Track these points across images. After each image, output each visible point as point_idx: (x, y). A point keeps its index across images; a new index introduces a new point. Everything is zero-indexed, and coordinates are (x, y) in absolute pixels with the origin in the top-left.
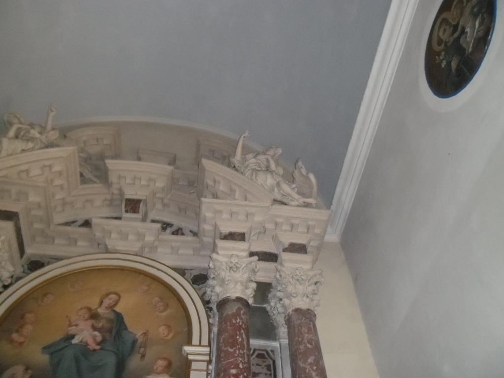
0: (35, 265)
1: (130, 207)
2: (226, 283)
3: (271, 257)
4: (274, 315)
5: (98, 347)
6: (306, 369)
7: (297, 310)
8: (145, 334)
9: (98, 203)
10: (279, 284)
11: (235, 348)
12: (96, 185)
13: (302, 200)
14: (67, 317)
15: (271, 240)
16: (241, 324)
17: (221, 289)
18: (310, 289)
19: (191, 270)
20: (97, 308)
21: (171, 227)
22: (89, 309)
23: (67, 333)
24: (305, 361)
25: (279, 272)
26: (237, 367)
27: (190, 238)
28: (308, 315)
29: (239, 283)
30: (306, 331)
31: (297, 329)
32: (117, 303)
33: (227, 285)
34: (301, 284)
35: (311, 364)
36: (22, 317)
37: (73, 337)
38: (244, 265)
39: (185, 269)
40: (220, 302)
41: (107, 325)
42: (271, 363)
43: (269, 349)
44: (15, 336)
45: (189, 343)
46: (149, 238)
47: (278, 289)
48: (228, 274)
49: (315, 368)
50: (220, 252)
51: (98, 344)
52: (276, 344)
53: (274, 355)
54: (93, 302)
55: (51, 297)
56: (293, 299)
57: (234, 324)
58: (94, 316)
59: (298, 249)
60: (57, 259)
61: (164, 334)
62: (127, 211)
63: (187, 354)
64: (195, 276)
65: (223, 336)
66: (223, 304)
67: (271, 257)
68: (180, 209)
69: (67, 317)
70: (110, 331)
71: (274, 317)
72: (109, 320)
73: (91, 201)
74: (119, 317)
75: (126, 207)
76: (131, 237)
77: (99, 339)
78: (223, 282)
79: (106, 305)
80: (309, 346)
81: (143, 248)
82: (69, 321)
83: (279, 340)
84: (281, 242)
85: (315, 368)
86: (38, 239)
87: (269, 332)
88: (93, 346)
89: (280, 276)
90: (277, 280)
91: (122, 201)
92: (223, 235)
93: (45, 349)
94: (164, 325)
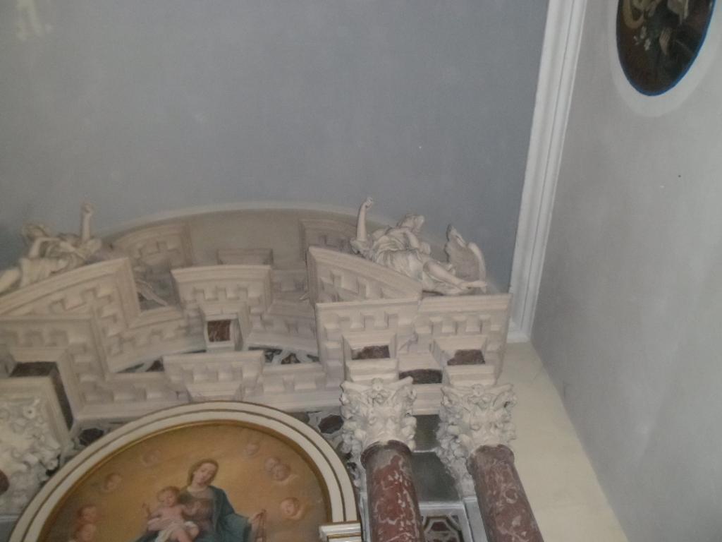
0: (90, 435)
1: (216, 333)
2: (371, 422)
3: (433, 377)
4: (450, 462)
6: (511, 536)
7: (484, 450)
8: (262, 515)
9: (169, 334)
10: (450, 413)
11: (398, 518)
12: (163, 309)
13: (465, 285)
14: (144, 505)
15: (428, 351)
16: (401, 480)
17: (364, 433)
18: (498, 415)
19: (316, 412)
20: (186, 487)
21: (279, 354)
22: (175, 490)
23: (147, 530)
24: (508, 526)
25: (447, 396)
27: (307, 366)
28: (501, 455)
29: (390, 421)
30: (502, 479)
31: (487, 477)
32: (213, 475)
33: (371, 425)
34: (482, 409)
35: (517, 528)
36: (80, 514)
37: (155, 534)
38: (393, 393)
39: (308, 412)
40: (365, 452)
41: (205, 510)
42: (456, 536)
43: (450, 515)
45: (328, 520)
46: (249, 374)
47: (450, 421)
48: (371, 409)
49: (524, 533)
50: (356, 378)
52: (459, 506)
53: (457, 521)
54: (180, 479)
55: (117, 479)
56: (475, 434)
57: (392, 483)
58: (183, 499)
60: (120, 423)
61: (289, 512)
62: (212, 340)
63: (328, 538)
64: (323, 420)
65: (378, 503)
66: (370, 454)
67: (433, 377)
68: (288, 326)
69: (144, 505)
70: (210, 518)
71: (450, 465)
72: (206, 502)
73: (159, 333)
74: (220, 496)
75: (209, 333)
76: (222, 376)
78: (365, 423)
79: (199, 481)
80: (510, 501)
81: (241, 389)
82: (148, 510)
83: (462, 498)
84: (443, 352)
85: (524, 533)
86: (90, 398)
87: (445, 488)
89: (450, 401)
90: (446, 408)
91: (203, 325)
92: (356, 353)
94: (287, 499)
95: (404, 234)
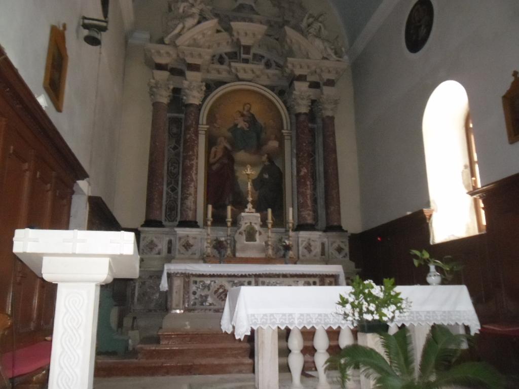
5: (248, 130)
7: (328, 117)
8: (265, 124)
22: (240, 112)
26: (305, 143)
28: (332, 119)
32: (250, 109)
44: (215, 125)
46: (258, 73)
51: (248, 128)
52: (315, 126)
54: (240, 108)
58: (243, 115)
59: (330, 83)
62: (244, 54)
66: (298, 115)
74: (253, 116)
77: (247, 125)
88: (246, 129)
91: (240, 48)
93: (229, 130)
95: (320, 27)
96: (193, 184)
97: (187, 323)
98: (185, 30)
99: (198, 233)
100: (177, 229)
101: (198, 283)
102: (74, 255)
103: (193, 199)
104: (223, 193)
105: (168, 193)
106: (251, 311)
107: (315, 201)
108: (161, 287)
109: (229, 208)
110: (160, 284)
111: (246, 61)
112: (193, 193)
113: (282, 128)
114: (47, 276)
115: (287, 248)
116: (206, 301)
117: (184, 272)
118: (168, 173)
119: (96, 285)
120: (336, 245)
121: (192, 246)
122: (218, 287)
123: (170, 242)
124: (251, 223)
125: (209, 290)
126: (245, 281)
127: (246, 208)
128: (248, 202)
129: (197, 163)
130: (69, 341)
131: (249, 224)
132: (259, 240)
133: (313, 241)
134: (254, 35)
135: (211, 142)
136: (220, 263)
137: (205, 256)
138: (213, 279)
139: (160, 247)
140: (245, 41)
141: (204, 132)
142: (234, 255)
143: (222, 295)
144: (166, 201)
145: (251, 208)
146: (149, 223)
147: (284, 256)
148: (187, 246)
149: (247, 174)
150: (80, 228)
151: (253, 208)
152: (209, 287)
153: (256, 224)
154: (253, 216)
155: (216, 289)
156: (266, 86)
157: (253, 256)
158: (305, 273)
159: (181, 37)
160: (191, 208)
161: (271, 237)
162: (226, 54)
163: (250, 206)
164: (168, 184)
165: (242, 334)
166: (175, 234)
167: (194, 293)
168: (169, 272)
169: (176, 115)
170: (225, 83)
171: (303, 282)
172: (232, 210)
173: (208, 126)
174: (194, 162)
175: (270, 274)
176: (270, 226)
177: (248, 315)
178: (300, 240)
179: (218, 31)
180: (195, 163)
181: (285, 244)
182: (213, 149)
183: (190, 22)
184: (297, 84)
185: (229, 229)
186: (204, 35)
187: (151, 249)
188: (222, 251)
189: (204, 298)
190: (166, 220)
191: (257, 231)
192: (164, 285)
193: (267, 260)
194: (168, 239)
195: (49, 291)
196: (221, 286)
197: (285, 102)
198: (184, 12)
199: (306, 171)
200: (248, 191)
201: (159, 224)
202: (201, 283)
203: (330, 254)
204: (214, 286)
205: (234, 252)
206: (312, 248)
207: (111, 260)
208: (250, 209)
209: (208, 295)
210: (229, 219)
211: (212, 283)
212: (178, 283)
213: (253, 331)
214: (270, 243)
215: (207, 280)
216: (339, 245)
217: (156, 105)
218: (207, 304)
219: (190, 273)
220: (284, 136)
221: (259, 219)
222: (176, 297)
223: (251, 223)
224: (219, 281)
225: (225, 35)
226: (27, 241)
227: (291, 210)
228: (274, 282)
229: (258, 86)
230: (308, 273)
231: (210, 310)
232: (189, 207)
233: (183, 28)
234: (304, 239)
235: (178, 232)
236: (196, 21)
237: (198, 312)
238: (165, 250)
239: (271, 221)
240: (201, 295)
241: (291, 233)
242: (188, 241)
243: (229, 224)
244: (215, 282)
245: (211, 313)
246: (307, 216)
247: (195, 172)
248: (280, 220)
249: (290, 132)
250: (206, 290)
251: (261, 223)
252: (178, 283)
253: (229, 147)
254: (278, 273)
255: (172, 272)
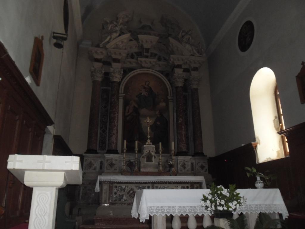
28: (197, 90)
32: (149, 84)
37: (141, 93)
44: (129, 93)
46: (154, 63)
58: (145, 88)
59: (196, 69)
62: (145, 53)
66: (177, 88)
74: (150, 88)
77: (147, 94)
96: (115, 128)
97: (111, 212)
98: (112, 40)
99: (118, 157)
100: (105, 155)
101: (118, 187)
102: (43, 170)
103: (115, 137)
104: (133, 134)
105: (100, 133)
106: (149, 205)
107: (187, 138)
108: (95, 189)
109: (137, 142)
110: (95, 188)
111: (147, 57)
112: (115, 133)
113: (168, 95)
114: (27, 182)
115: (171, 166)
116: (122, 198)
117: (109, 181)
118: (101, 122)
119: (56, 189)
120: (200, 164)
121: (114, 165)
122: (130, 190)
123: (101, 163)
124: (149, 151)
125: (124, 191)
126: (146, 186)
127: (147, 142)
128: (148, 139)
129: (118, 116)
130: (39, 223)
131: (148, 152)
132: (154, 162)
133: (186, 162)
134: (151, 42)
135: (126, 103)
136: (131, 175)
137: (122, 171)
138: (127, 185)
139: (95, 165)
140: (146, 46)
141: (122, 98)
142: (140, 170)
143: (132, 195)
144: (100, 138)
145: (150, 142)
146: (89, 151)
147: (169, 171)
148: (112, 165)
149: (147, 122)
150: (48, 154)
151: (151, 142)
152: (124, 189)
153: (152, 151)
154: (151, 147)
155: (129, 191)
156: (158, 71)
157: (151, 171)
158: (182, 181)
159: (109, 44)
160: (114, 142)
161: (161, 160)
162: (135, 53)
163: (149, 141)
164: (101, 128)
165: (144, 219)
166: (104, 157)
167: (116, 193)
168: (101, 181)
169: (105, 88)
170: (134, 69)
171: (181, 187)
172: (138, 143)
173: (124, 94)
174: (116, 115)
175: (160, 182)
176: (161, 152)
177: (147, 207)
178: (179, 161)
179: (131, 40)
180: (117, 116)
181: (169, 164)
182: (128, 107)
183: (114, 35)
184: (176, 70)
185: (136, 155)
186: (122, 42)
187: (90, 167)
188: (132, 168)
189: (121, 196)
190: (99, 150)
191: (153, 156)
192: (97, 188)
193: (159, 174)
194: (100, 160)
195: (29, 191)
196: (132, 189)
197: (169, 80)
198: (111, 29)
199: (182, 120)
200: (148, 132)
201: (94, 151)
202: (120, 187)
203: (197, 169)
204: (127, 190)
205: (139, 168)
206: (186, 166)
207: (65, 173)
208: (149, 143)
209: (124, 195)
210: (137, 149)
211: (126, 187)
212: (106, 187)
213: (150, 217)
214: (161, 163)
215: (123, 186)
216: (202, 165)
217: (94, 82)
218: (123, 200)
219: (113, 181)
220: (169, 99)
221: (155, 149)
222: (104, 196)
223: (149, 151)
224: (130, 186)
225: (134, 42)
226: (16, 162)
227: (173, 143)
228: (163, 187)
229: (153, 71)
230: (184, 181)
231: (125, 204)
232: (113, 142)
233: (111, 38)
234: (181, 161)
235: (106, 157)
236: (118, 34)
237: (118, 205)
238: (98, 167)
239: (161, 150)
240: (119, 195)
241: (173, 157)
242: (112, 162)
243: (136, 152)
244: (128, 187)
245: (126, 206)
246: (182, 147)
247: (117, 121)
248: (167, 149)
249: (173, 97)
250: (123, 191)
251: (156, 151)
252: (106, 187)
253: (136, 106)
254: (165, 181)
255: (102, 180)
